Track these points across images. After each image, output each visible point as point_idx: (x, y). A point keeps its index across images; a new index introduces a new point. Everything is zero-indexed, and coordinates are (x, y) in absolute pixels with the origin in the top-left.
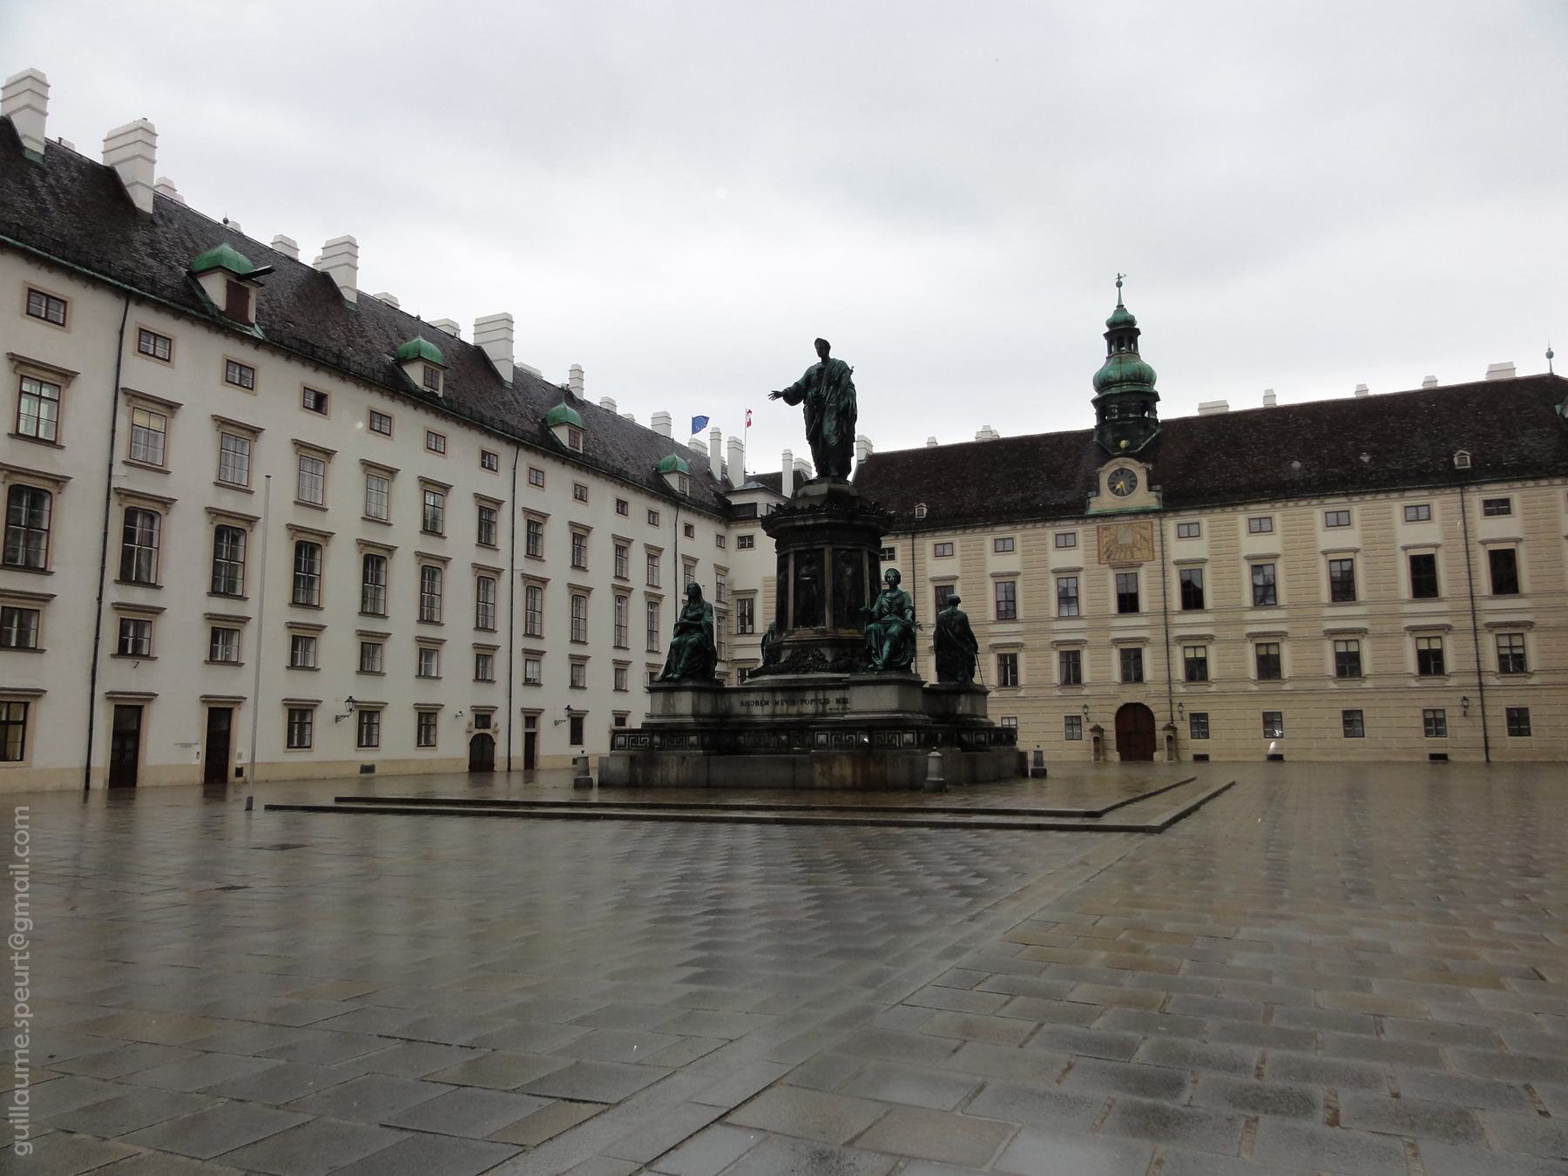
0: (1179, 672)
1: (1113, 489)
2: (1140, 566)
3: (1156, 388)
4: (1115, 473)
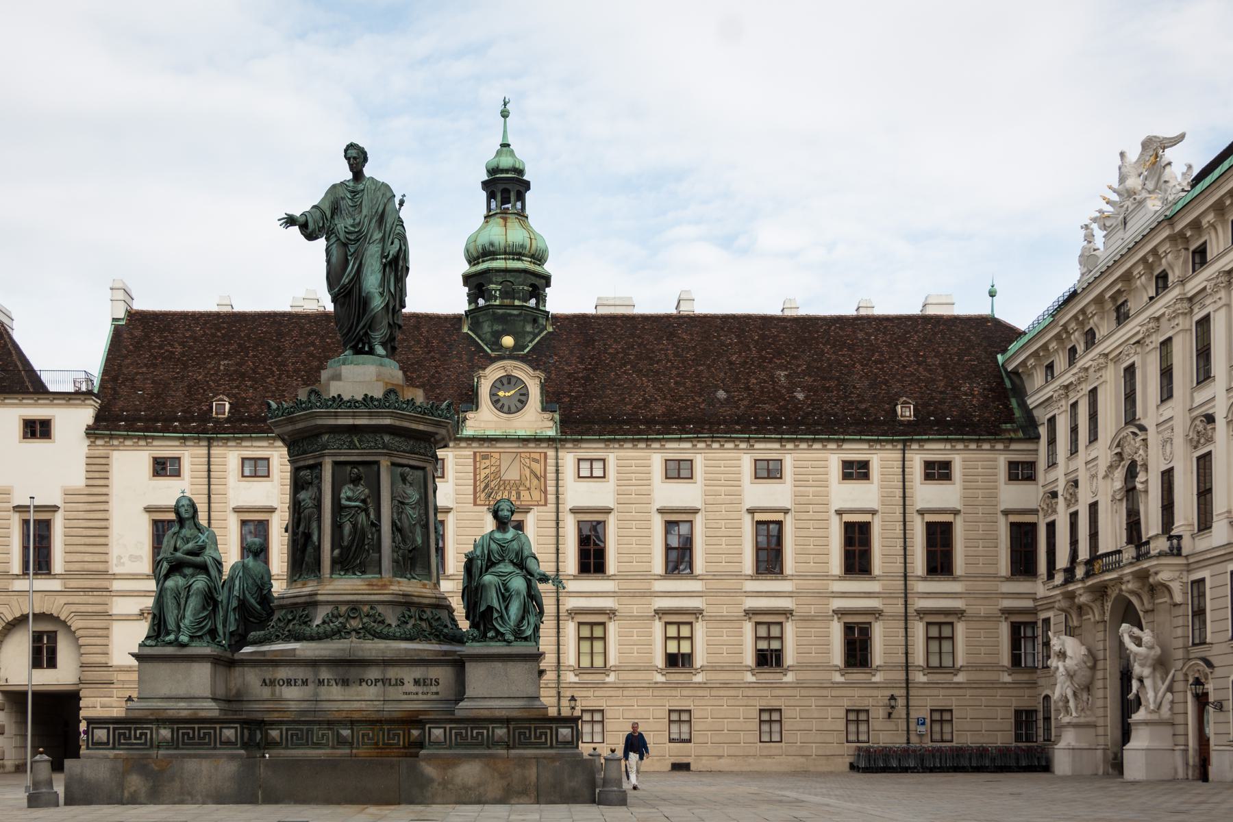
1: (496, 402)
3: (548, 267)
4: (500, 380)
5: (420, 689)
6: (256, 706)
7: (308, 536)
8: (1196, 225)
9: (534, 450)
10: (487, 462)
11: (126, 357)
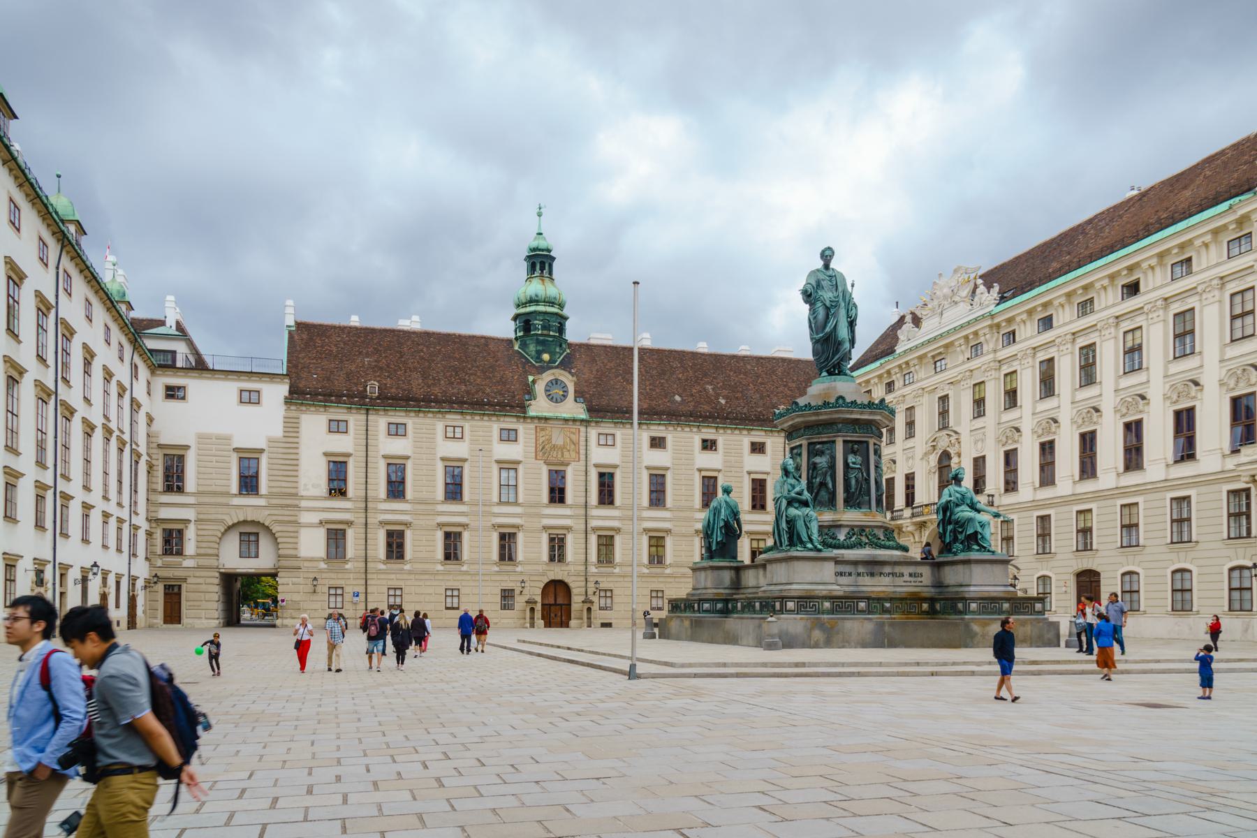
0: (593, 557)
2: (567, 465)
3: (565, 312)
5: (912, 579)
6: (951, 589)
7: (823, 484)
8: (1010, 321)
9: (574, 427)
10: (543, 433)
11: (300, 352)
